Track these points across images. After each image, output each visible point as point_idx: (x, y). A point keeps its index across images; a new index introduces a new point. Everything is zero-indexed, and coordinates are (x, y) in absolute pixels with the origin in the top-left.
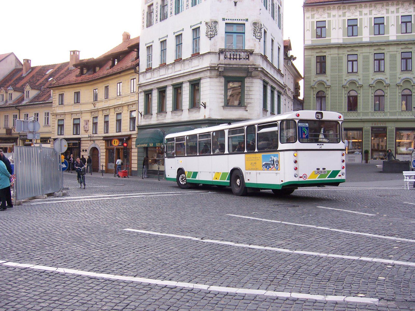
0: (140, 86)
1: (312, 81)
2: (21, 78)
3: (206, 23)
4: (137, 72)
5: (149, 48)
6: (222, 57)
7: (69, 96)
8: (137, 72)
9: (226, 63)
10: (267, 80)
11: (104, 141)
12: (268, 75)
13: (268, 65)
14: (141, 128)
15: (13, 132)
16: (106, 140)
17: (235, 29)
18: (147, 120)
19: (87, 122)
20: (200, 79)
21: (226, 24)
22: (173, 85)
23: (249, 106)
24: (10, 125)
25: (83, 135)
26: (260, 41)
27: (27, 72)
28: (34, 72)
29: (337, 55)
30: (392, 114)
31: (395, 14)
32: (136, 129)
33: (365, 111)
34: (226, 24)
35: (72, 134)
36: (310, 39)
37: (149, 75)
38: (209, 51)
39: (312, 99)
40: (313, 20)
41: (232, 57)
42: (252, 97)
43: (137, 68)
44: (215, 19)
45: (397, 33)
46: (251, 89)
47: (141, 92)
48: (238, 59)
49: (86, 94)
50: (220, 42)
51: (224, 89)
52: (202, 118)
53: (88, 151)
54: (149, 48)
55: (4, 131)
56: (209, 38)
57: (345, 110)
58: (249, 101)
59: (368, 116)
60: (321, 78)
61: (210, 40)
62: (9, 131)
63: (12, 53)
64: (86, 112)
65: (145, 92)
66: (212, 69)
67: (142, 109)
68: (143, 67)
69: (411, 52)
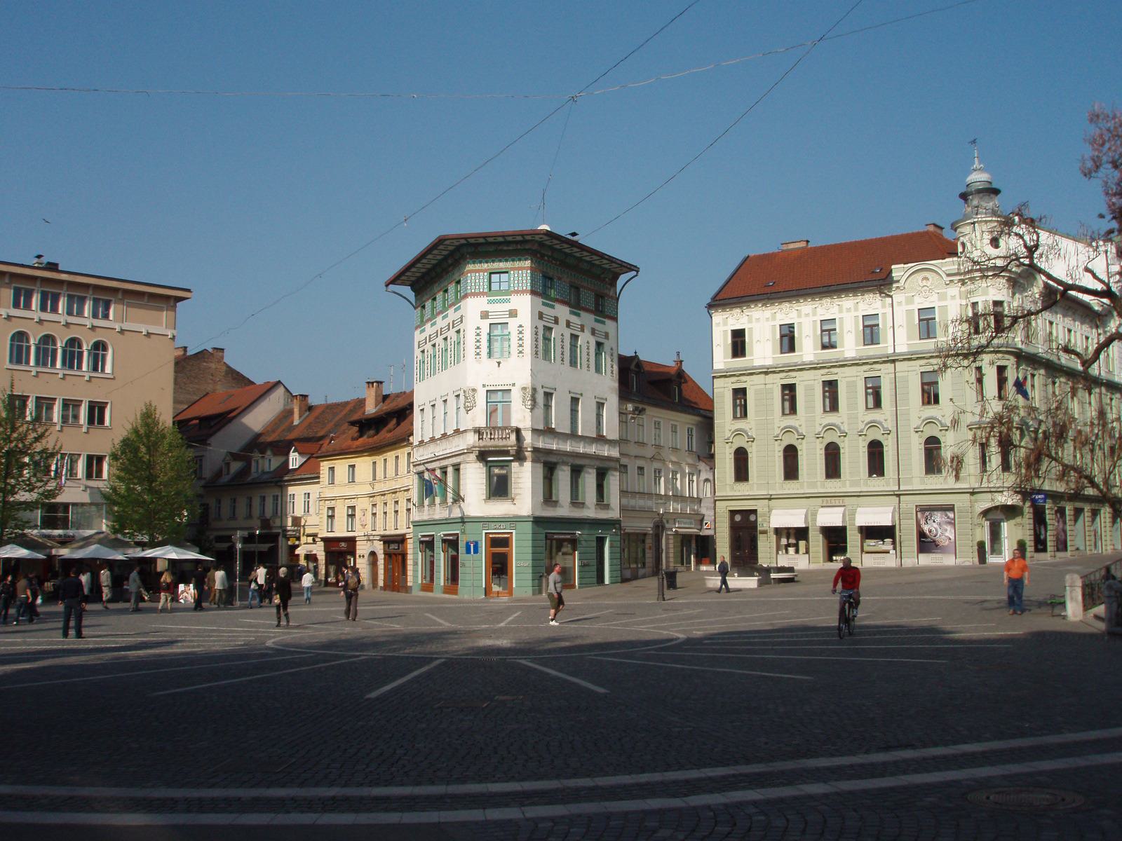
3: (464, 392)
6: (477, 436)
9: (481, 445)
10: (553, 459)
11: (382, 542)
14: (417, 524)
16: (385, 542)
19: (364, 511)
21: (487, 391)
22: (441, 468)
25: (358, 533)
27: (300, 417)
28: (316, 413)
29: (763, 386)
30: (853, 484)
31: (853, 314)
32: (411, 526)
34: (487, 391)
35: (346, 530)
39: (728, 460)
44: (473, 386)
45: (856, 346)
46: (520, 475)
48: (496, 440)
53: (366, 556)
58: (518, 491)
60: (741, 424)
61: (467, 413)
63: (279, 382)
64: (363, 496)
66: (470, 451)
68: (415, 439)
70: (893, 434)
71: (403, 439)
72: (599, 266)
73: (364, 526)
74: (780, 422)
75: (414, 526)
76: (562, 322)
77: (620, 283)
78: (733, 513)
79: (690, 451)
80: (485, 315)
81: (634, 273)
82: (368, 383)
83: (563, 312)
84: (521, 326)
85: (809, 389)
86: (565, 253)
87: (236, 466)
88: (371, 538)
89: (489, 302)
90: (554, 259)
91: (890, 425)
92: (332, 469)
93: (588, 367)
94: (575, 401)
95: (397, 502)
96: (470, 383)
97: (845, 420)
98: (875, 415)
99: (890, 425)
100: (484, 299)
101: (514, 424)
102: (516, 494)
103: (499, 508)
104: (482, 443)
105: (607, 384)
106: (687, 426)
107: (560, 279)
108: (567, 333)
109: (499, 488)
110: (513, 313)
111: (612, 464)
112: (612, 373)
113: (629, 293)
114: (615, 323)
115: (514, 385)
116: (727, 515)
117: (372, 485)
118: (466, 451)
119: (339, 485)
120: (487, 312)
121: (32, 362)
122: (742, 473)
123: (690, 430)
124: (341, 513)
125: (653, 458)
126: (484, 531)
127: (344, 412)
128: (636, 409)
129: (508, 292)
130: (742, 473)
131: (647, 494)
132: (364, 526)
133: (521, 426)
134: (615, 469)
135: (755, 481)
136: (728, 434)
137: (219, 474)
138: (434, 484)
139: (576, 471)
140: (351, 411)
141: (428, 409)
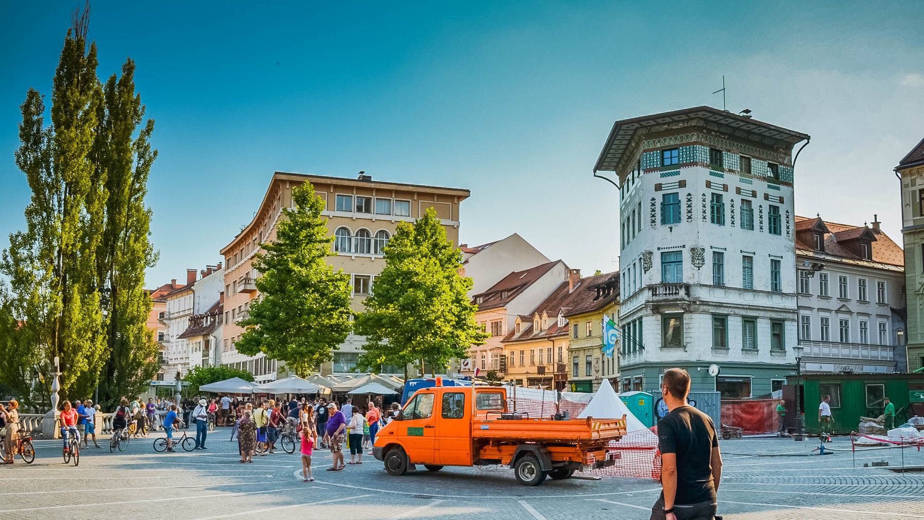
2: (567, 295)
6: (651, 293)
8: (618, 303)
14: (622, 369)
15: (546, 370)
17: (671, 259)
21: (662, 253)
24: (545, 363)
34: (662, 253)
36: (911, 218)
40: (914, 188)
42: (691, 335)
44: (649, 249)
50: (655, 276)
55: (535, 370)
62: (541, 370)
63: (560, 261)
68: (621, 298)
72: (771, 137)
73: (597, 371)
76: (732, 189)
77: (794, 152)
79: (881, 304)
80: (658, 187)
81: (806, 141)
83: (732, 180)
84: (689, 195)
86: (733, 127)
87: (524, 326)
89: (662, 176)
90: (722, 133)
93: (761, 228)
94: (748, 260)
96: (645, 248)
100: (658, 173)
101: (684, 281)
102: (687, 343)
103: (674, 355)
104: (655, 298)
105: (783, 246)
106: (876, 281)
107: (729, 151)
108: (738, 200)
109: (674, 338)
110: (682, 184)
111: (790, 316)
112: (788, 233)
113: (805, 164)
114: (790, 188)
115: (684, 246)
119: (581, 339)
120: (661, 184)
121: (353, 250)
123: (881, 286)
125: (838, 311)
128: (814, 265)
129: (678, 166)
131: (832, 342)
132: (597, 371)
133: (691, 282)
134: (793, 320)
136: (918, 287)
137: (513, 333)
138: (632, 335)
139: (750, 323)
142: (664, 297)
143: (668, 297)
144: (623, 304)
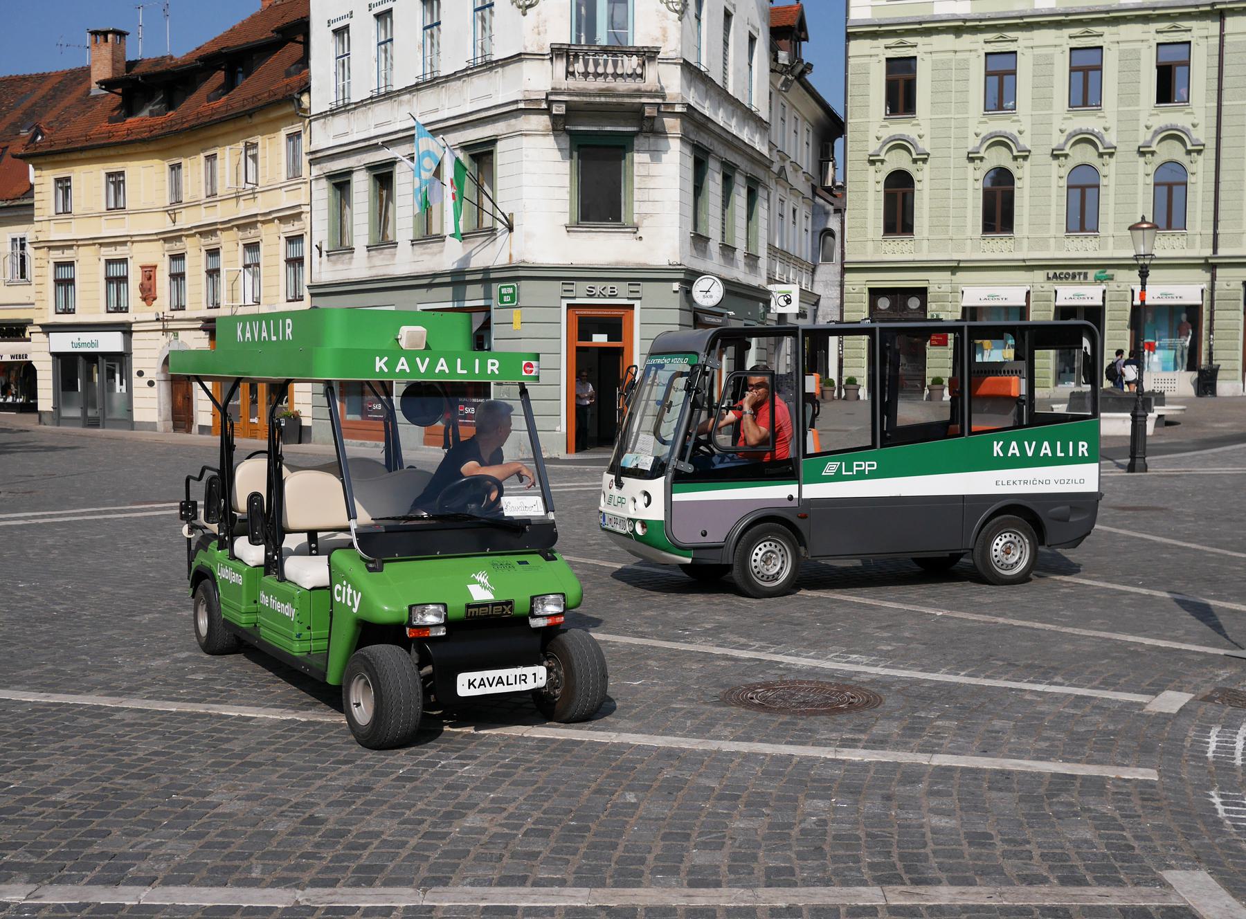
0: (316, 158)
1: (872, 138)
4: (302, 114)
5: (341, 32)
7: (88, 179)
10: (706, 141)
12: (710, 125)
13: (712, 93)
14: (320, 291)
18: (340, 267)
20: (493, 142)
23: (646, 223)
26: (680, 19)
32: (306, 293)
33: (1038, 235)
37: (339, 123)
38: (523, 51)
39: (871, 195)
41: (591, 69)
43: (305, 98)
47: (318, 178)
49: (146, 177)
51: (568, 171)
52: (502, 261)
54: (341, 32)
56: (520, 7)
57: (973, 232)
59: (1048, 248)
61: (524, 14)
64: (147, 238)
65: (330, 177)
67: (319, 228)
68: (320, 98)
69: (1189, 43)
70: (1210, 153)
71: (287, 102)
74: (977, 123)
75: (312, 295)
78: (875, 293)
82: (95, 33)
85: (1042, 64)
88: (172, 325)
91: (1203, 134)
92: (64, 185)
95: (213, 253)
97: (1112, 122)
98: (1171, 116)
99: (1203, 134)
103: (602, 248)
104: (572, 84)
116: (866, 297)
117: (172, 212)
118: (522, 106)
122: (899, 219)
124: (90, 272)
126: (565, 302)
127: (40, 93)
130: (899, 219)
135: (926, 235)
140: (54, 89)
141: (365, 32)
142: (600, 84)
143: (611, 83)
144: (333, 113)
